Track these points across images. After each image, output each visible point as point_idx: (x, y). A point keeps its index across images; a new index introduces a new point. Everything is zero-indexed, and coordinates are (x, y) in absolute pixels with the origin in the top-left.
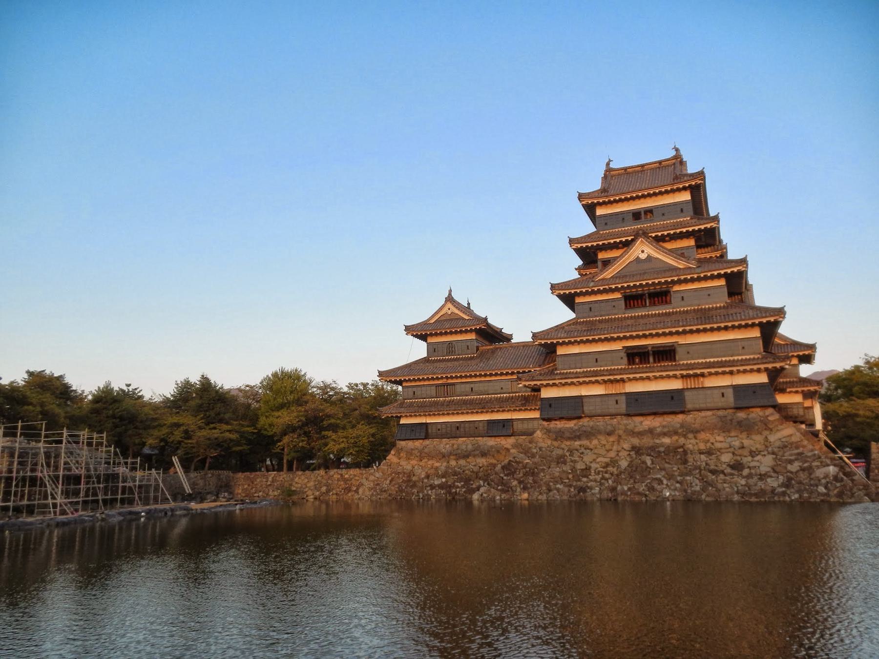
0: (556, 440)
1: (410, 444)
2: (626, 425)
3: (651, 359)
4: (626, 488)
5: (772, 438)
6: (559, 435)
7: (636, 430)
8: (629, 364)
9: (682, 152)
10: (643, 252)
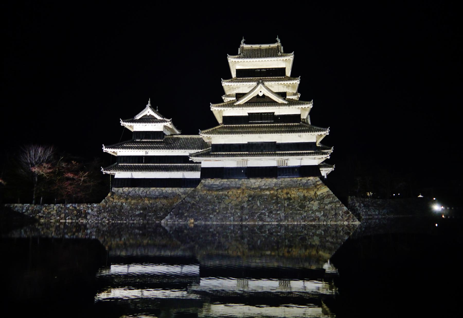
0: (209, 190)
5: (318, 193)
6: (210, 188)
7: (252, 187)
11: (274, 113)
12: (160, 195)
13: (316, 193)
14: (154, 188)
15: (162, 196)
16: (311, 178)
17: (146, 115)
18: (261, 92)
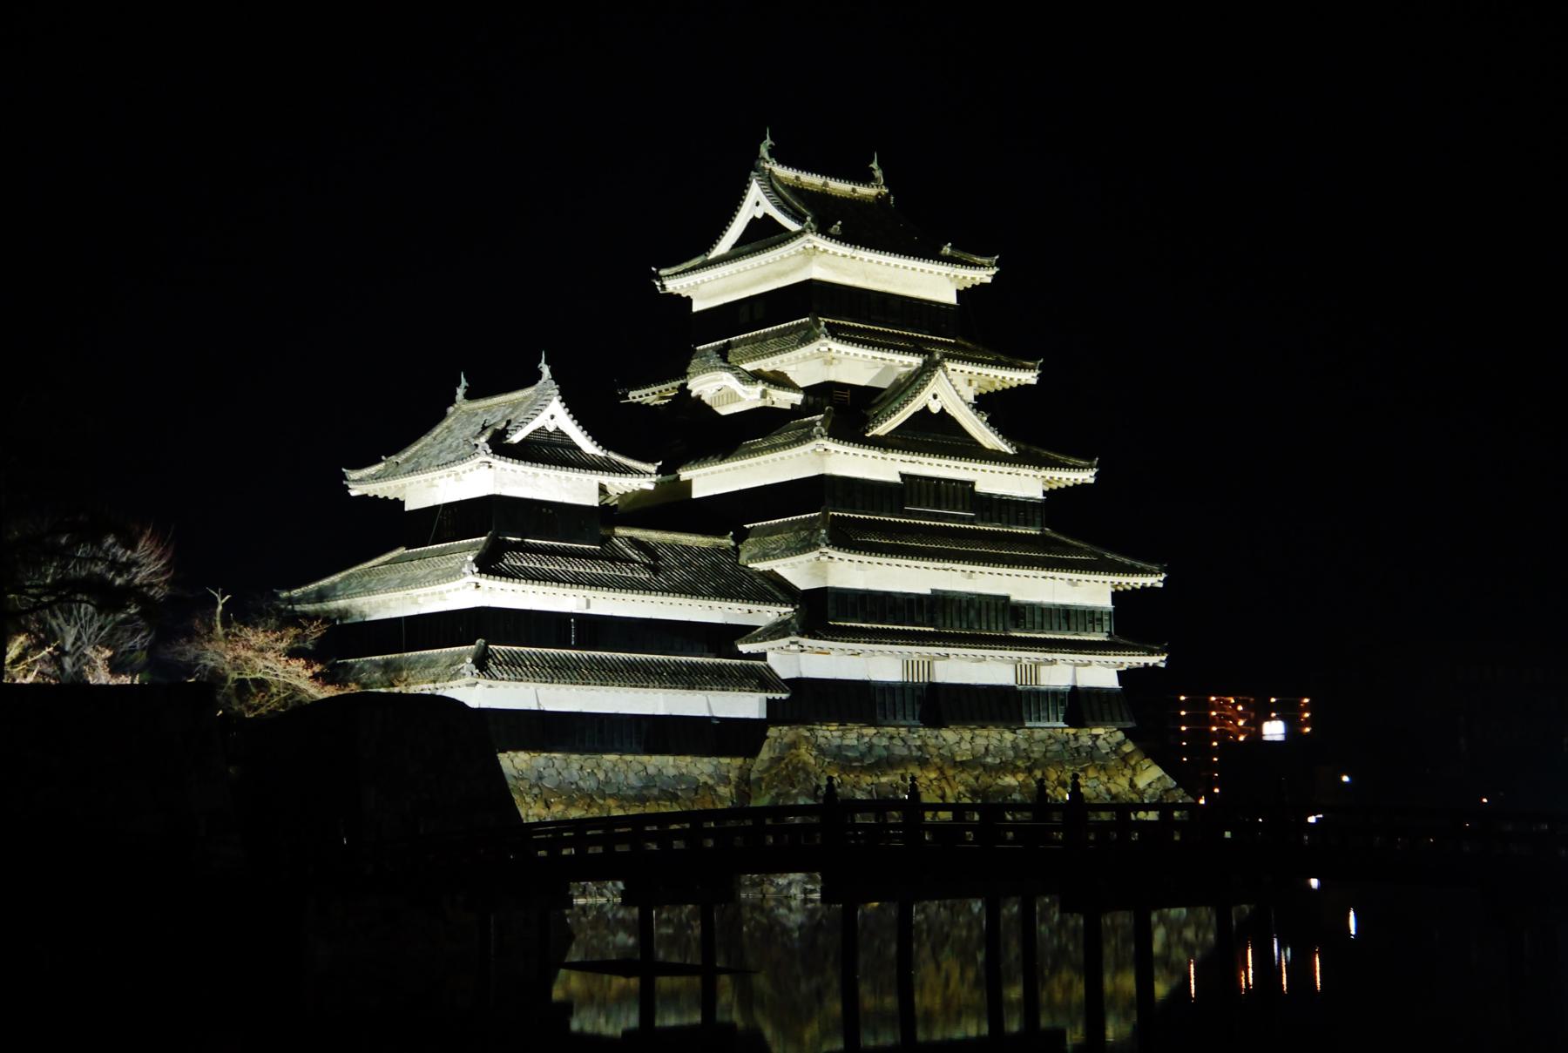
5: (1141, 783)
6: (842, 759)
11: (973, 483)
12: (646, 787)
13: (1132, 785)
14: (613, 757)
15: (655, 792)
16: (1099, 731)
17: (542, 429)
18: (935, 397)
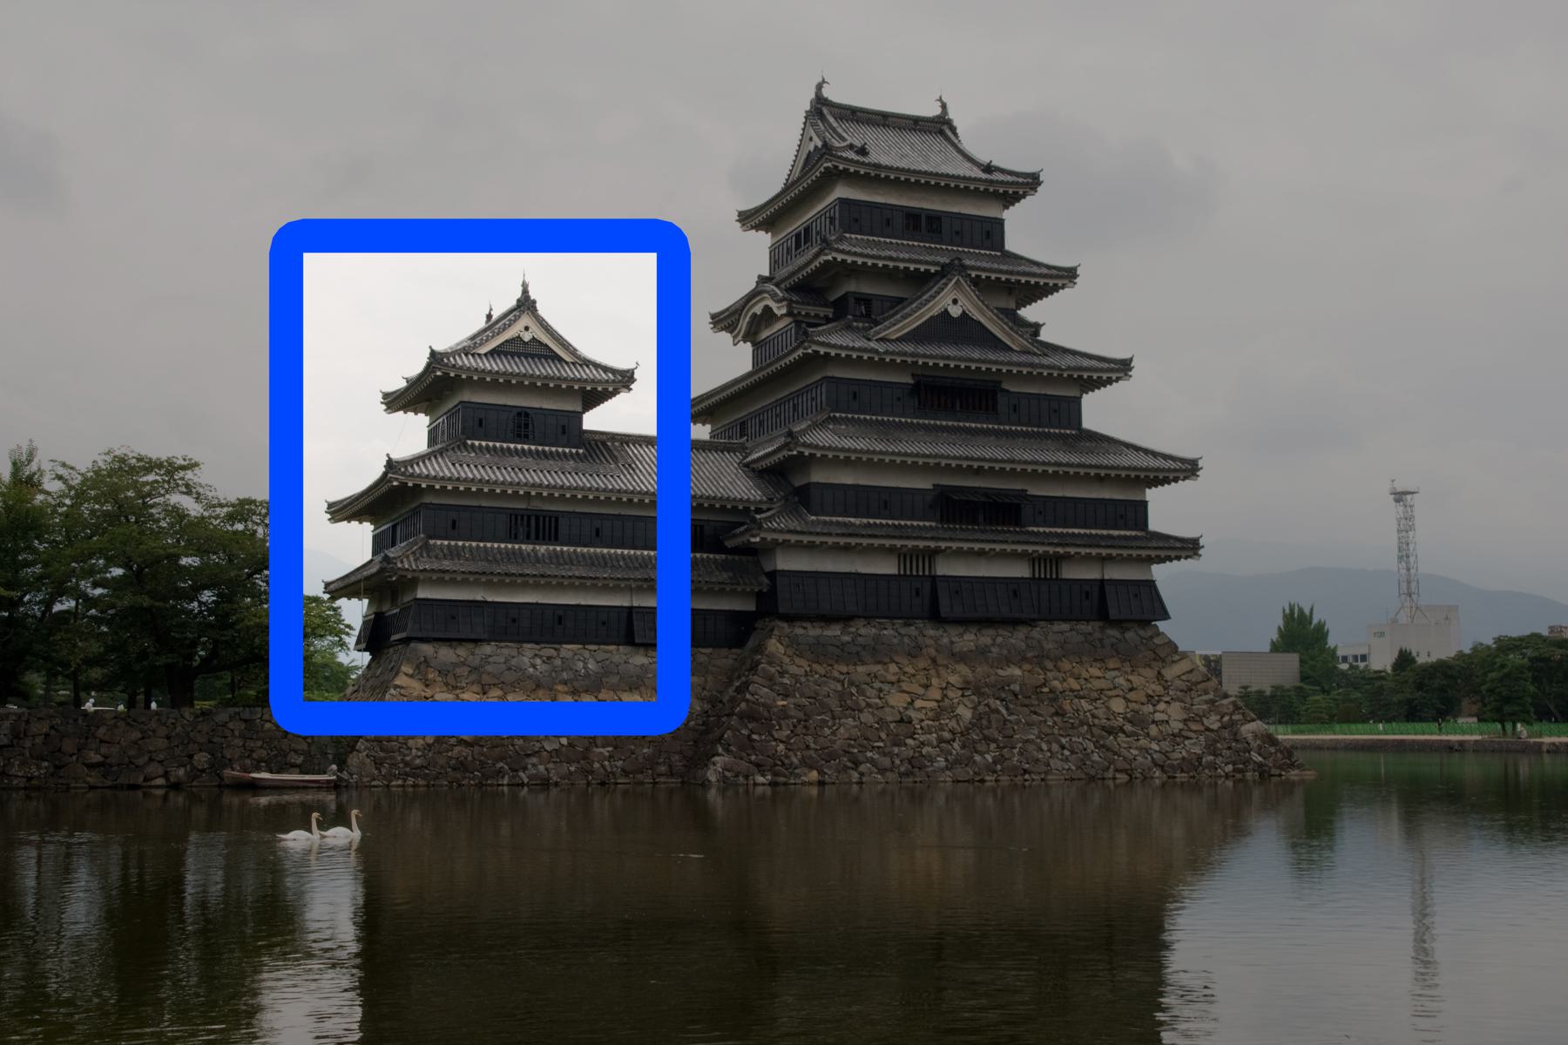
1: (446, 654)
2: (936, 640)
3: (981, 518)
4: (989, 758)
5: (1170, 673)
8: (941, 521)
9: (952, 115)
10: (955, 302)
18: (955, 302)
